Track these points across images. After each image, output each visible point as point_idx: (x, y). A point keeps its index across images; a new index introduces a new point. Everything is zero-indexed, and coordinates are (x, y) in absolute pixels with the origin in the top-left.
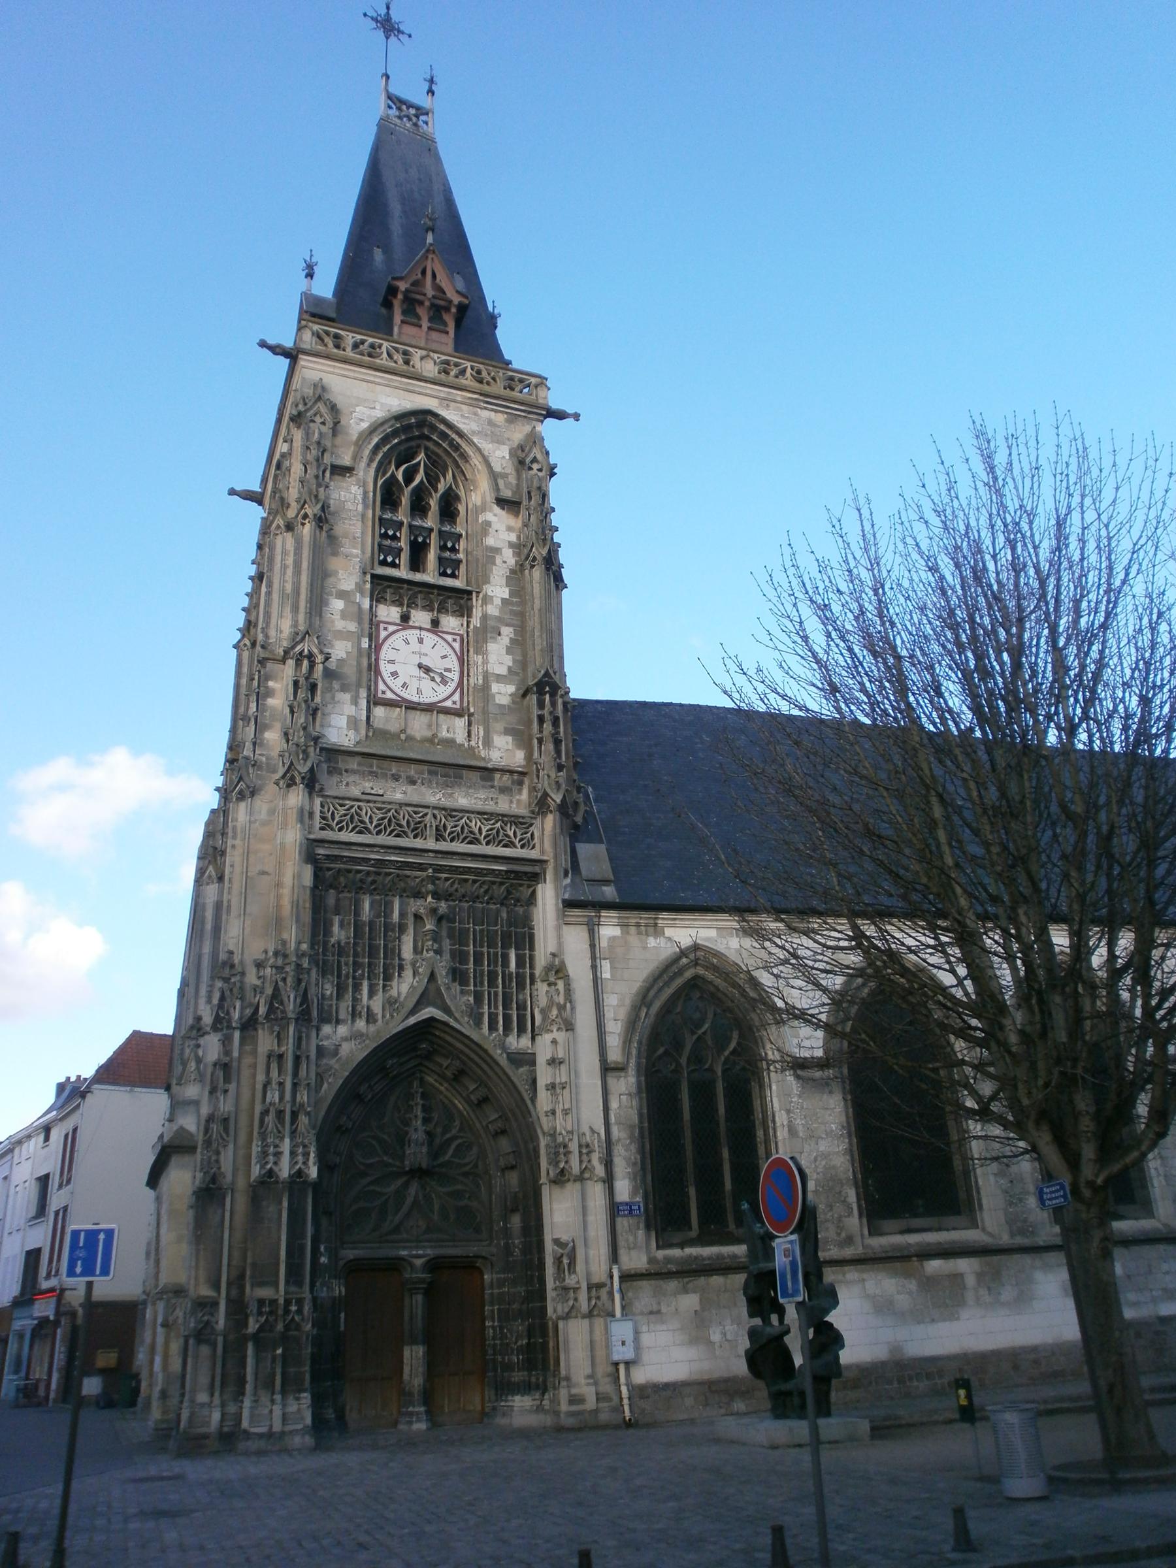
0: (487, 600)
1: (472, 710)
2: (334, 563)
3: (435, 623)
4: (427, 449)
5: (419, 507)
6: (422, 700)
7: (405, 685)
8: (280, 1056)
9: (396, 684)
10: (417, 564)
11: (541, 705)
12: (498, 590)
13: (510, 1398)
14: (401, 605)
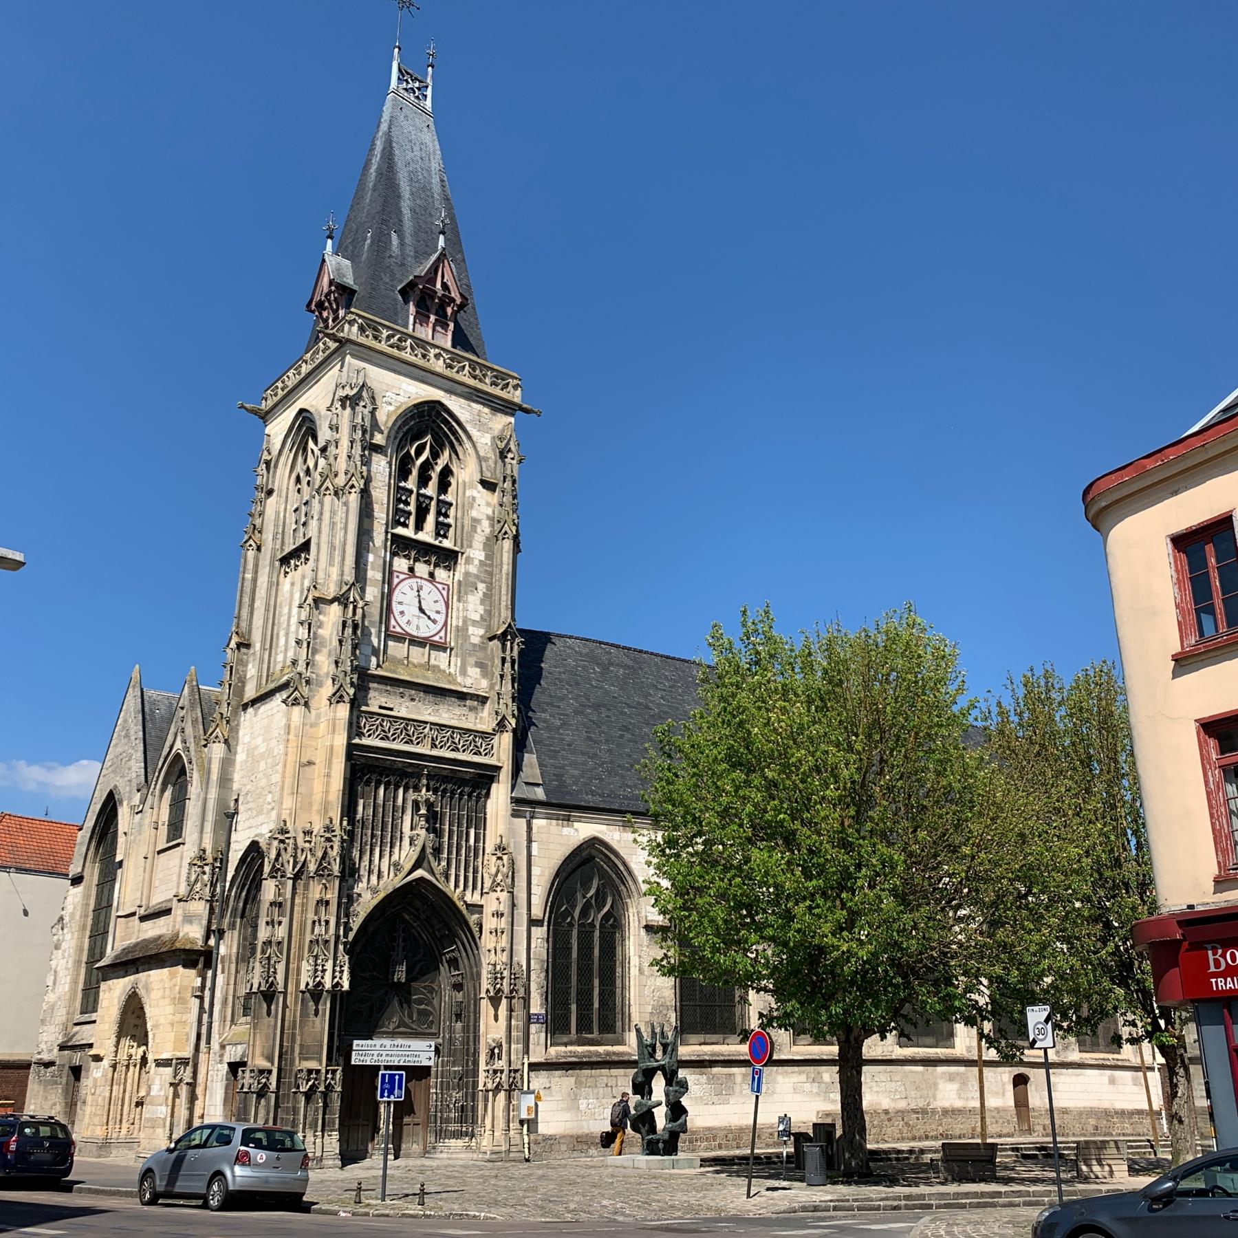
0: (469, 560)
1: (453, 644)
3: (432, 575)
4: (432, 429)
5: (424, 480)
6: (419, 635)
7: (408, 622)
8: (327, 903)
9: (402, 621)
10: (419, 527)
11: (504, 650)
12: (476, 553)
13: (447, 1140)
14: (409, 559)
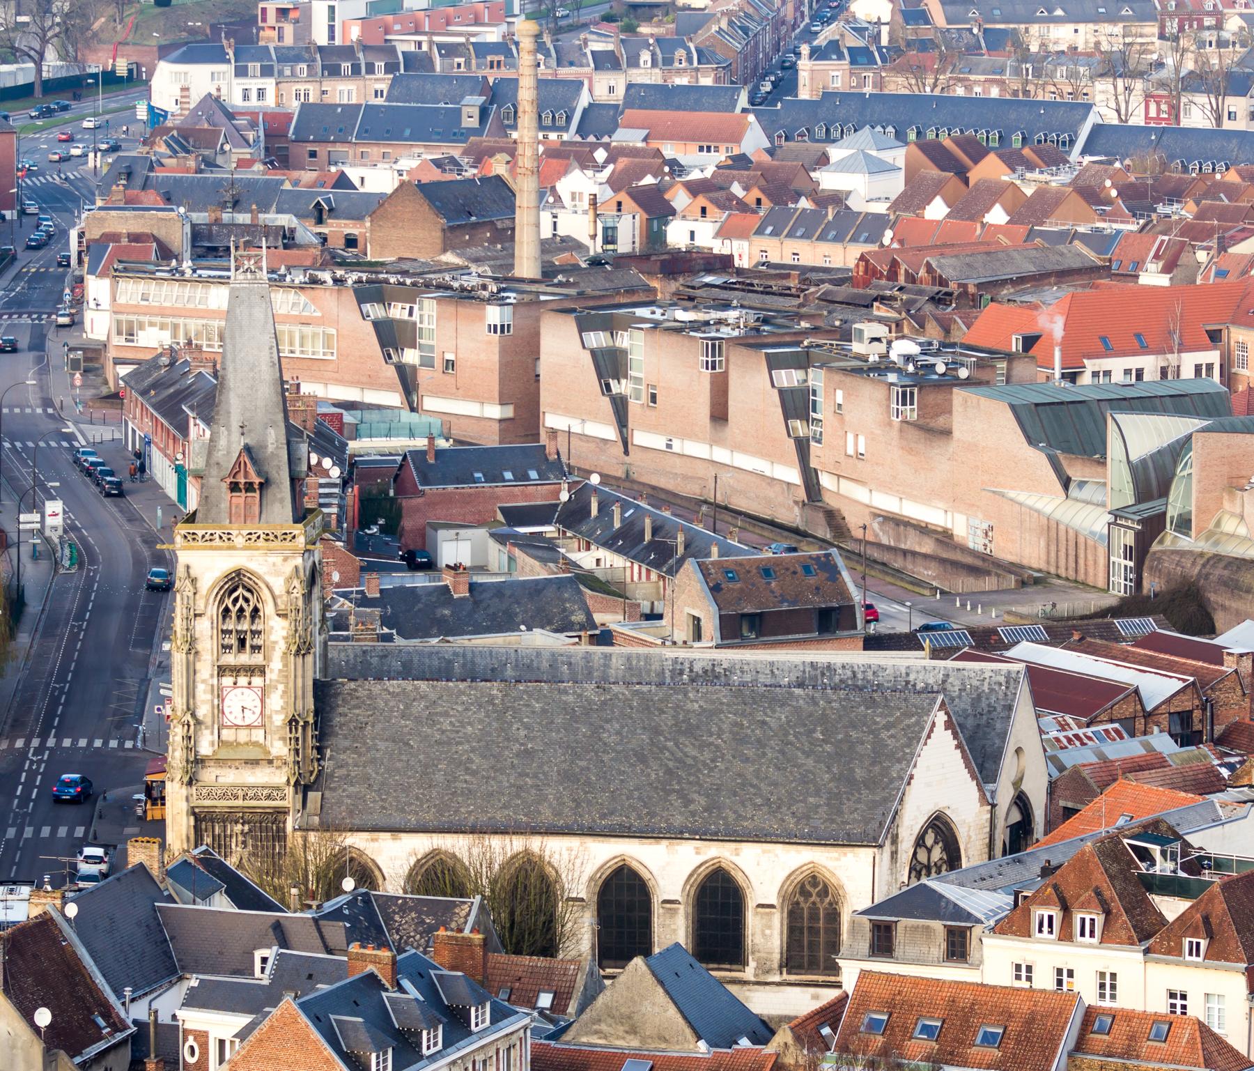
2: (199, 666)
9: (231, 717)
